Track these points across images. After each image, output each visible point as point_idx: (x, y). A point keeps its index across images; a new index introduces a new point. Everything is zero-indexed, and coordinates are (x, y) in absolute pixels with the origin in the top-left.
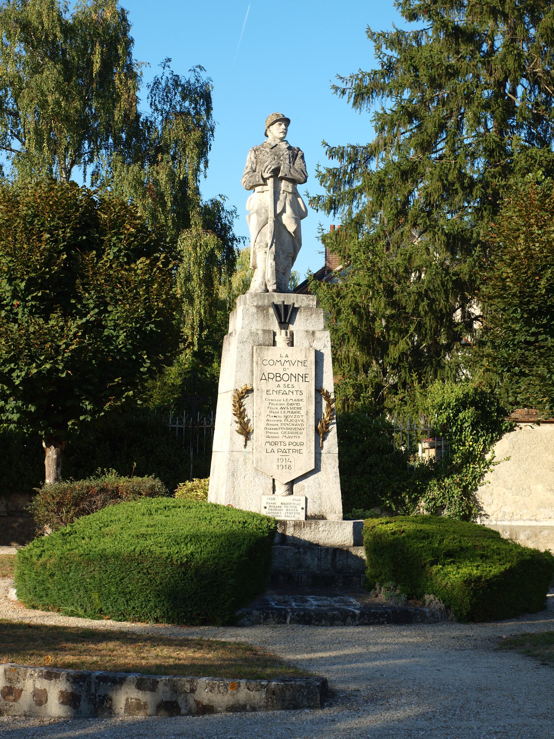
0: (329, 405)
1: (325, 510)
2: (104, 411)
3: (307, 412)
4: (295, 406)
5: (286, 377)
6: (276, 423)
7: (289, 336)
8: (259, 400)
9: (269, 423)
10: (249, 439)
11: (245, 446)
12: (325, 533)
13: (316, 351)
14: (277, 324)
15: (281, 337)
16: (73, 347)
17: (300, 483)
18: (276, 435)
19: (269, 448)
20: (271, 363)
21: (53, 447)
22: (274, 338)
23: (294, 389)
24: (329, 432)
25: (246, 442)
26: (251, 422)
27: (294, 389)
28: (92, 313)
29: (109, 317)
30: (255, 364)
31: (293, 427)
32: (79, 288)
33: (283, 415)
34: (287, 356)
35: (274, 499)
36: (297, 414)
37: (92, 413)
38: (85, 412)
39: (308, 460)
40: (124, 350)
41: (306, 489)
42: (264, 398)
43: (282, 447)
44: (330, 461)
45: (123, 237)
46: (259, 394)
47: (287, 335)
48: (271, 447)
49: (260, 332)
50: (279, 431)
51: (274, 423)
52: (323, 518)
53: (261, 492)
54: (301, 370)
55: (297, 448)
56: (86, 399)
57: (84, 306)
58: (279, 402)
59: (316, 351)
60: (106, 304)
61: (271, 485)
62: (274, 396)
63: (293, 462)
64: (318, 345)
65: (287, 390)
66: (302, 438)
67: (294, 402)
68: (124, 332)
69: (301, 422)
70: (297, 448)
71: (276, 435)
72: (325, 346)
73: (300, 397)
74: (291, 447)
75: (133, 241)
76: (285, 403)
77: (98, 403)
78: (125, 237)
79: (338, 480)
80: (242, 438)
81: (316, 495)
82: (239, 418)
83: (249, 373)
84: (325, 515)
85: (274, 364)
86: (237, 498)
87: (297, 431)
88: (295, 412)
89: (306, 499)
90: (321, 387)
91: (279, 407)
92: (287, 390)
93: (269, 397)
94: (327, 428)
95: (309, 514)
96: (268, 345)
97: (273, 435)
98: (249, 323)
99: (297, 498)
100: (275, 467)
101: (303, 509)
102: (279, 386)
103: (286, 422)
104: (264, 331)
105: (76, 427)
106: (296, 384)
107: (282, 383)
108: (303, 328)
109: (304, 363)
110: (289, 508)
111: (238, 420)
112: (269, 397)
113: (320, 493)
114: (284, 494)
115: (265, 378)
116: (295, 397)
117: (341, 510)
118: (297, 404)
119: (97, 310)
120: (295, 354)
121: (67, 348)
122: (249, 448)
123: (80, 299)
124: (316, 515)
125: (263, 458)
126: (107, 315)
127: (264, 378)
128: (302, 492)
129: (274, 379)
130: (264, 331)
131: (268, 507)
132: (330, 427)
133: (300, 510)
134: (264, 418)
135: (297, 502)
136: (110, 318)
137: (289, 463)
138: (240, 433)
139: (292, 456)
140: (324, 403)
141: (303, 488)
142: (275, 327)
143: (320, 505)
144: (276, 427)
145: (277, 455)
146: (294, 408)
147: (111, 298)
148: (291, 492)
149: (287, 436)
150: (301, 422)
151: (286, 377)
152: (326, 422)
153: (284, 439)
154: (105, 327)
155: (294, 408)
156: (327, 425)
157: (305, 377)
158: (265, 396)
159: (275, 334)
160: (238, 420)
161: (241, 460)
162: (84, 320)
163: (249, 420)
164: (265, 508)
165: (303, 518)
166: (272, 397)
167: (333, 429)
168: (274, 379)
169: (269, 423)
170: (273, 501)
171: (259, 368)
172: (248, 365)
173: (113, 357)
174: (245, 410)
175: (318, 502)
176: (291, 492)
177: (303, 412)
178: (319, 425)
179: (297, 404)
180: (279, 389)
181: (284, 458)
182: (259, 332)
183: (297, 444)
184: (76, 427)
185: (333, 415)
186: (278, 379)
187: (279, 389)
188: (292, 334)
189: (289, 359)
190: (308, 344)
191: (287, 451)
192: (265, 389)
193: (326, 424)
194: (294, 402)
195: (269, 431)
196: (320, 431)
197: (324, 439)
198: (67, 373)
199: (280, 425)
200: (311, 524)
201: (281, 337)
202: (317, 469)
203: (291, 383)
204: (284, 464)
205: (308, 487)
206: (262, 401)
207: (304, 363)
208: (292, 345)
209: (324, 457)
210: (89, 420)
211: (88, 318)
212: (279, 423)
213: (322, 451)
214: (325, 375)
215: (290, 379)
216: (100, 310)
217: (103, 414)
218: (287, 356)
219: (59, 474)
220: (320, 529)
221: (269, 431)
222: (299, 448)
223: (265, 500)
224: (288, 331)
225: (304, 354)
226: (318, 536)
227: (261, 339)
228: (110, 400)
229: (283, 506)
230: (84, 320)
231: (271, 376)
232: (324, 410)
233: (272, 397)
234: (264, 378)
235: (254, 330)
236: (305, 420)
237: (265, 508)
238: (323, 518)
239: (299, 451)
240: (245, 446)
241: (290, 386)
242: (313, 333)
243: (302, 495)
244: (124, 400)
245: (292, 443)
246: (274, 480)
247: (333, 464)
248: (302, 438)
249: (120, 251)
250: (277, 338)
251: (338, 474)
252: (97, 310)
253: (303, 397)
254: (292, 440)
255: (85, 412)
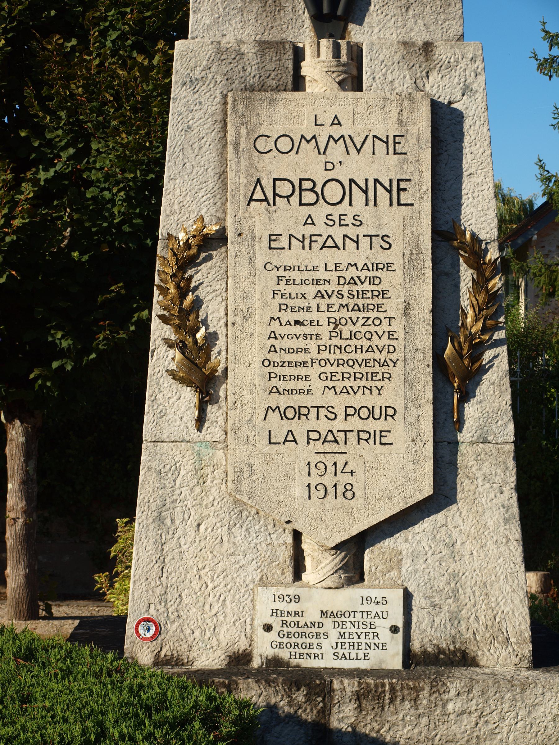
0: (480, 283)
1: (473, 630)
2: (97, 350)
3: (407, 307)
4: (366, 286)
5: (333, 192)
6: (301, 343)
7: (344, 58)
8: (244, 270)
9: (278, 343)
10: (214, 400)
11: (200, 421)
12: (468, 722)
13: (435, 106)
14: (308, 22)
15: (317, 67)
16: (16, 223)
17: (388, 543)
18: (302, 385)
19: (279, 428)
20: (284, 144)
21: (18, 423)
22: (297, 68)
23: (361, 231)
24: (483, 370)
25: (202, 410)
26: (221, 343)
27: (361, 231)
28: (64, 156)
29: (95, 162)
30: (230, 149)
31: (360, 356)
32: (32, 106)
33: (323, 318)
34: (336, 121)
35: (297, 599)
36: (373, 314)
37: (77, 354)
38: (61, 354)
39: (410, 466)
40: (126, 228)
41: (407, 564)
42: (259, 265)
43: (323, 426)
44: (486, 468)
45: (128, 10)
46: (244, 249)
47: (337, 54)
48: (286, 425)
49: (249, 50)
50: (313, 372)
51: (294, 344)
52: (463, 659)
53: (252, 573)
54: (385, 167)
55: (372, 425)
56: (58, 328)
57: (50, 144)
58: (310, 276)
59: (435, 106)
60: (87, 137)
61: (285, 553)
62: (294, 255)
63: (359, 474)
64: (442, 87)
65: (338, 233)
66: (392, 394)
67: (363, 275)
68: (119, 191)
69: (385, 340)
70: (372, 425)
71: (302, 385)
72: (466, 90)
73: (382, 258)
74: (354, 423)
75: (150, 17)
76: (333, 276)
77: (84, 337)
78: (132, 10)
79: (515, 532)
80: (189, 397)
81: (441, 583)
82: (178, 328)
83: (212, 182)
84: (472, 648)
85: (295, 148)
86: (172, 595)
87: (373, 370)
88: (366, 308)
89: (408, 597)
90: (456, 222)
91: (311, 290)
92: (338, 233)
93: (276, 258)
94: (476, 356)
95: (416, 646)
96: (277, 89)
97: (291, 385)
98: (216, 22)
99: (375, 593)
100: (300, 491)
101: (394, 629)
102: (309, 221)
103: (335, 341)
104: (264, 46)
105: (49, 384)
106: (367, 214)
107: (320, 212)
108: (393, 35)
109: (394, 144)
110: (349, 628)
111: (173, 337)
112: (276, 258)
113: (455, 577)
114: (329, 583)
115: (264, 194)
116: (363, 255)
117: (528, 634)
118: (372, 281)
119: (71, 151)
120: (363, 114)
121: (7, 224)
122: (213, 430)
123: (38, 130)
124: (441, 651)
125: (257, 461)
126: (91, 160)
127: (258, 195)
128: (394, 574)
129: (295, 199)
130: (264, 46)
131: (277, 627)
132: (488, 355)
133: (385, 635)
134: (260, 331)
135: (374, 609)
136: (98, 165)
137: (345, 479)
138: (182, 381)
139: (357, 454)
140: (466, 275)
141: (396, 561)
142: (303, 33)
143: (454, 618)
144: (301, 357)
145: (304, 453)
146: (362, 293)
147: (98, 126)
148: (352, 571)
149: (339, 385)
150: (385, 340)
151: (333, 192)
152: (472, 337)
153: (330, 398)
154: (89, 184)
155: (362, 293)
156: (477, 349)
157: (397, 190)
158: (262, 256)
159: (298, 55)
160: (173, 337)
161: (186, 469)
162: (52, 173)
163: (211, 338)
164: (268, 628)
165: (395, 662)
166: (288, 258)
167: (498, 365)
168: (295, 199)
169: (278, 343)
170: (293, 607)
171: (244, 164)
172: (210, 155)
173: (111, 244)
174: (198, 303)
175: (449, 605)
176: (352, 571)
177: (393, 306)
178: (449, 350)
179: (372, 281)
180: (310, 230)
181: (329, 460)
182: (244, 48)
183: (371, 412)
184: (49, 384)
185: (495, 315)
186: (309, 197)
187: (310, 230)
188: (356, 54)
189: (345, 130)
190: (408, 82)
191: (340, 437)
192: (262, 231)
193: (473, 347)
194: (363, 275)
195: (279, 370)
196: (452, 367)
197: (466, 395)
198: (10, 276)
199: (314, 350)
200: (417, 690)
201: (317, 67)
202: (443, 495)
203: (351, 212)
204: (329, 480)
205: (415, 556)
206: (253, 273)
207: (394, 144)
208: (360, 89)
209: (466, 455)
210: (69, 368)
211: (57, 168)
212: (312, 345)
213: (461, 437)
214: (467, 185)
215: (347, 195)
216: (78, 150)
217: (93, 356)
218: (336, 121)
219: (31, 472)
220: (450, 707)
221: (279, 370)
222: (380, 425)
223: (265, 604)
224: (343, 44)
225: (394, 115)
226: (442, 730)
227: (252, 70)
228: (103, 328)
229: (328, 622)
230: (52, 173)
231: (284, 189)
232: (465, 301)
233: (288, 258)
234: (258, 195)
235: (229, 40)
236: (400, 333)
237: (268, 628)
238: (463, 659)
239: (380, 438)
240: (200, 421)
241: (349, 220)
242: (427, 47)
243: (394, 585)
244: (132, 328)
245: (357, 412)
246: (297, 536)
247: (498, 480)
248: (392, 394)
249: (123, 37)
250: (306, 69)
251: (515, 510)
252: (71, 151)
253: (394, 256)
254: (357, 401)
255: (61, 354)
